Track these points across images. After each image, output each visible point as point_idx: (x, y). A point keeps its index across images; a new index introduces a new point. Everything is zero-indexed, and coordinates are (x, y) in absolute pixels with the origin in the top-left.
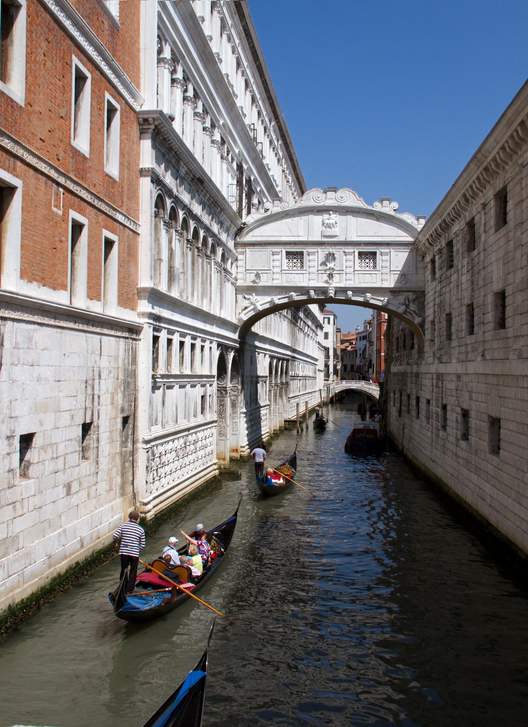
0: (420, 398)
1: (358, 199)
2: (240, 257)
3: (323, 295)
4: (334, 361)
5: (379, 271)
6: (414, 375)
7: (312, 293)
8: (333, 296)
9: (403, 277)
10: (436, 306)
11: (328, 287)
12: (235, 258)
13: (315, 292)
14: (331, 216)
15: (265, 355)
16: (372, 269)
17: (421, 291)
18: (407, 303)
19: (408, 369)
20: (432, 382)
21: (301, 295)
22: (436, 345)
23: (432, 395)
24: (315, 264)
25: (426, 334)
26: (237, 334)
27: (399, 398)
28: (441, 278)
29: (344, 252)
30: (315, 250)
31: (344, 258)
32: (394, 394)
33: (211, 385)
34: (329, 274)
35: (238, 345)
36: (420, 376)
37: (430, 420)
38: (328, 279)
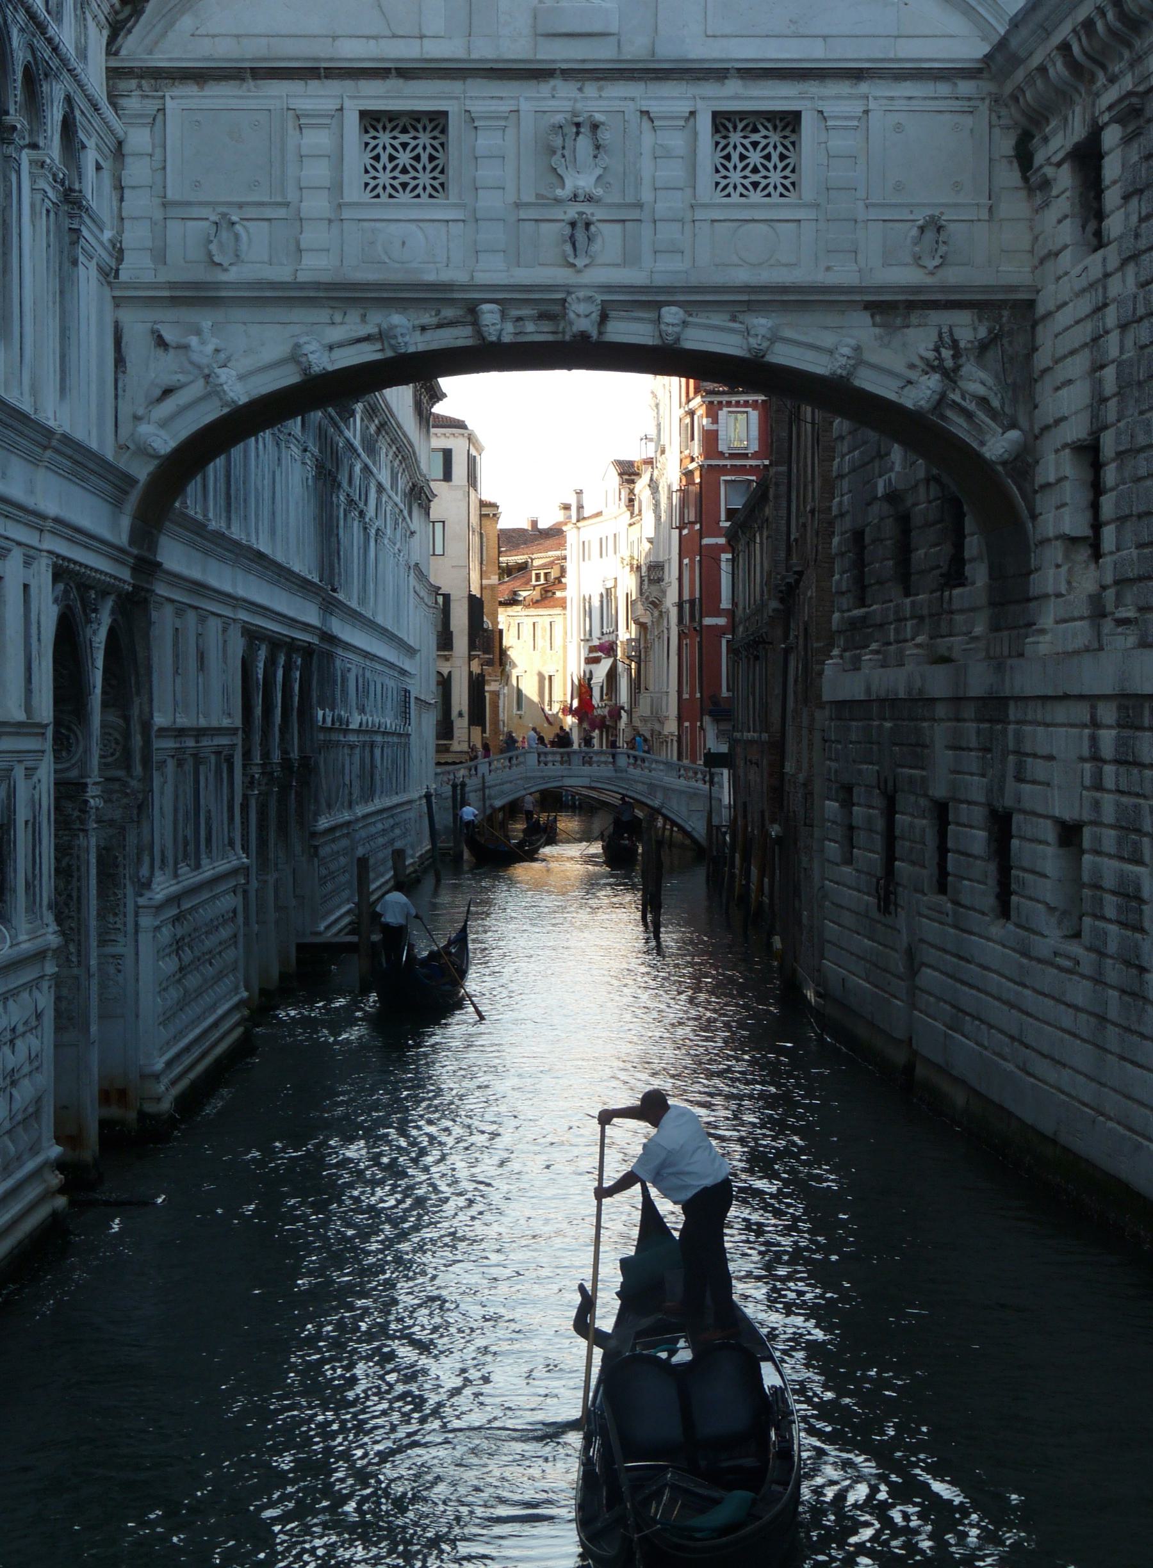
0: (1017, 818)
2: (139, 139)
4: (471, 658)
6: (969, 711)
7: (489, 314)
9: (930, 235)
10: (1110, 373)
11: (568, 289)
12: (112, 144)
15: (227, 623)
17: (1016, 305)
18: (949, 363)
19: (938, 683)
20: (1094, 740)
21: (440, 326)
22: (1107, 561)
23: (1096, 805)
25: (1045, 504)
26: (126, 522)
27: (880, 824)
28: (1137, 236)
30: (505, 107)
31: (648, 139)
32: (847, 804)
33: (30, 772)
34: (573, 224)
35: (125, 574)
36: (1013, 713)
37: (1087, 920)
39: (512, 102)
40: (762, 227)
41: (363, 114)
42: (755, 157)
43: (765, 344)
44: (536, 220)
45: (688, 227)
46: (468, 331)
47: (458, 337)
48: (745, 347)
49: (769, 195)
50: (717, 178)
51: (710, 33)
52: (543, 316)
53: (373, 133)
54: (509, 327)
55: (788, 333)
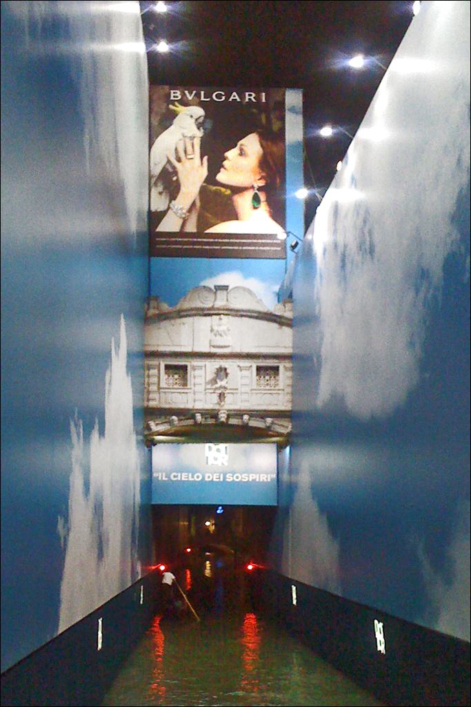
5: (283, 390)
7: (199, 417)
14: (223, 321)
16: (272, 388)
24: (203, 382)
29: (239, 366)
31: (239, 372)
34: (220, 394)
41: (167, 367)
42: (267, 377)
46: (192, 421)
52: (212, 417)
54: (204, 419)
55: (276, 422)
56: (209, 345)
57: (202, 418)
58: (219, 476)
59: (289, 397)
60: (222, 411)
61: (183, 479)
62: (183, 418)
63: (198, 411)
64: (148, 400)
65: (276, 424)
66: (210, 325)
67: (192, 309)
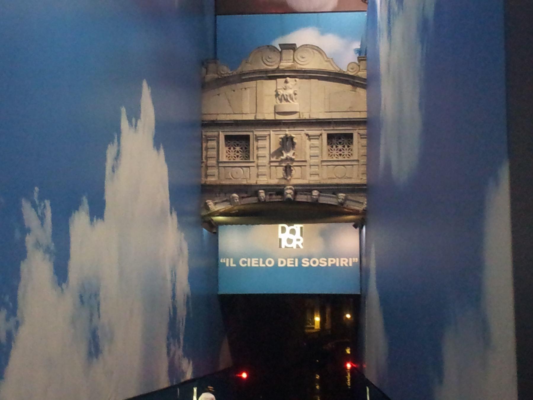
1: (326, 59)
3: (280, 197)
5: (358, 161)
7: (262, 194)
8: (292, 199)
11: (284, 186)
13: (266, 191)
24: (266, 152)
29: (307, 135)
34: (286, 167)
38: (285, 174)
39: (269, 132)
40: (342, 167)
42: (340, 147)
43: (343, 201)
44: (276, 166)
45: (320, 166)
46: (256, 198)
47: (253, 200)
48: (337, 202)
49: (344, 158)
50: (329, 153)
51: (326, 111)
53: (229, 141)
54: (268, 197)
55: (350, 197)
56: (273, 112)
57: (266, 194)
58: (294, 261)
59: (363, 169)
60: (288, 187)
61: (253, 265)
62: (246, 195)
63: (262, 187)
64: (207, 176)
65: (348, 200)
66: (275, 89)
67: (254, 72)
